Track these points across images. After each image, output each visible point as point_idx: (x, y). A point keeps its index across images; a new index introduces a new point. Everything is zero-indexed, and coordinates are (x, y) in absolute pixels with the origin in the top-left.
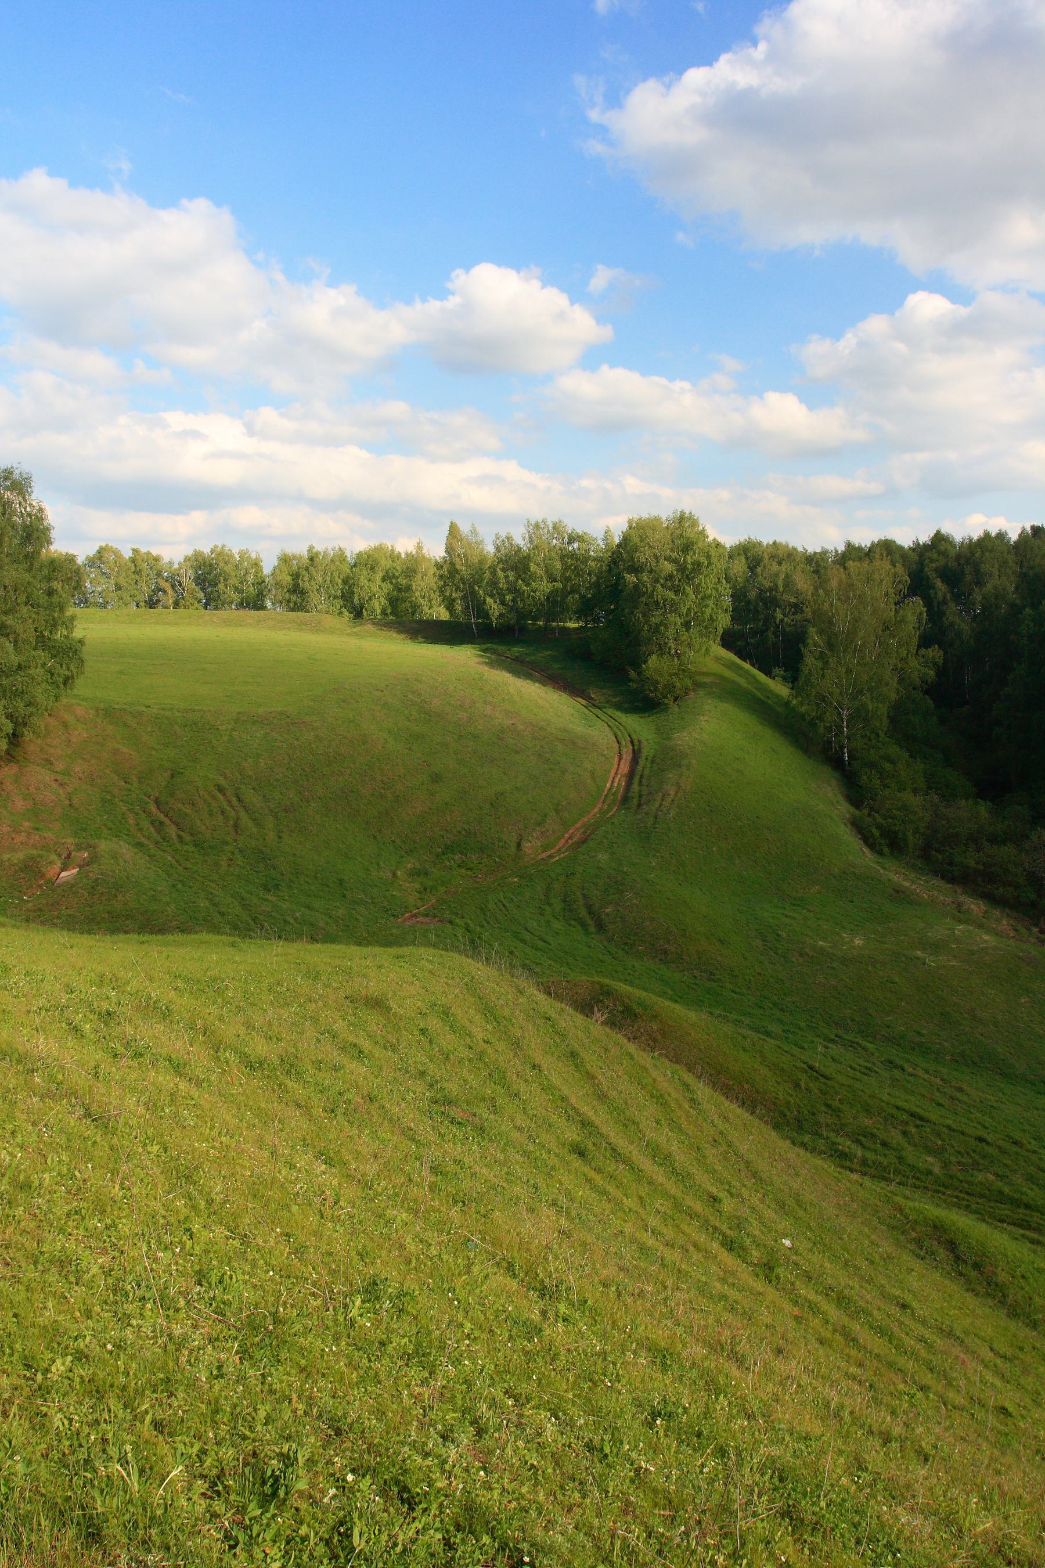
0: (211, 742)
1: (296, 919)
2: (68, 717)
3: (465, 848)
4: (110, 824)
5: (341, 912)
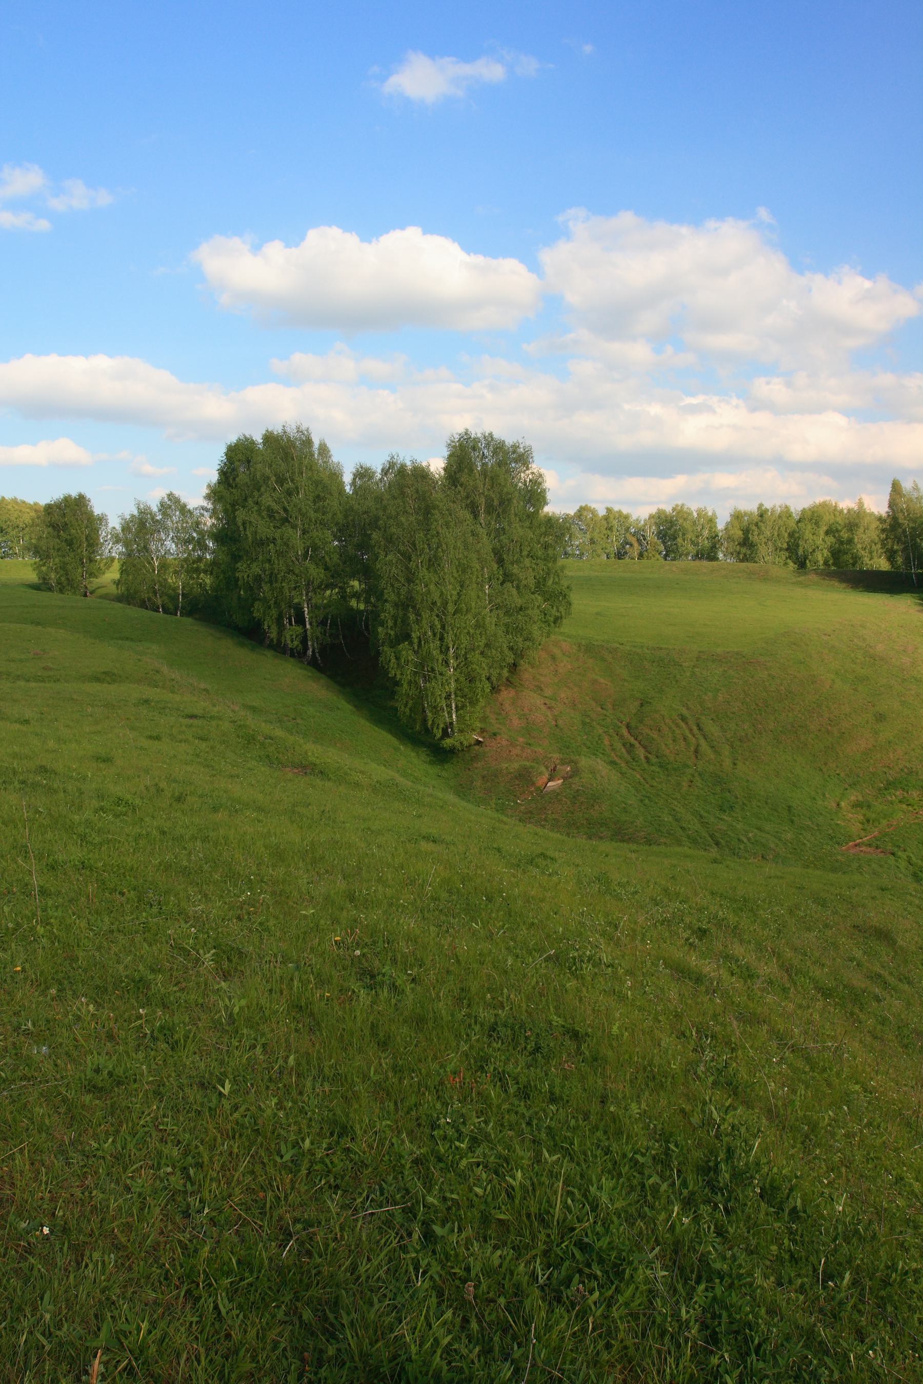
0: (675, 677)
1: (749, 839)
2: (556, 651)
3: (907, 785)
4: (589, 744)
5: (789, 836)
